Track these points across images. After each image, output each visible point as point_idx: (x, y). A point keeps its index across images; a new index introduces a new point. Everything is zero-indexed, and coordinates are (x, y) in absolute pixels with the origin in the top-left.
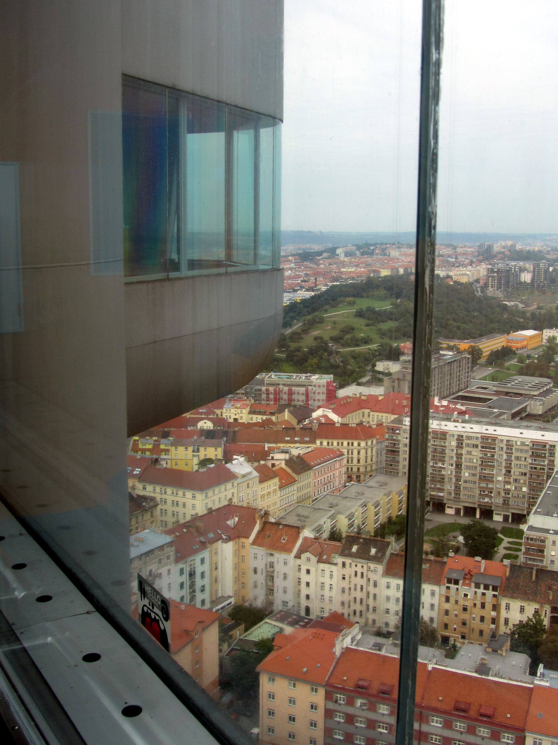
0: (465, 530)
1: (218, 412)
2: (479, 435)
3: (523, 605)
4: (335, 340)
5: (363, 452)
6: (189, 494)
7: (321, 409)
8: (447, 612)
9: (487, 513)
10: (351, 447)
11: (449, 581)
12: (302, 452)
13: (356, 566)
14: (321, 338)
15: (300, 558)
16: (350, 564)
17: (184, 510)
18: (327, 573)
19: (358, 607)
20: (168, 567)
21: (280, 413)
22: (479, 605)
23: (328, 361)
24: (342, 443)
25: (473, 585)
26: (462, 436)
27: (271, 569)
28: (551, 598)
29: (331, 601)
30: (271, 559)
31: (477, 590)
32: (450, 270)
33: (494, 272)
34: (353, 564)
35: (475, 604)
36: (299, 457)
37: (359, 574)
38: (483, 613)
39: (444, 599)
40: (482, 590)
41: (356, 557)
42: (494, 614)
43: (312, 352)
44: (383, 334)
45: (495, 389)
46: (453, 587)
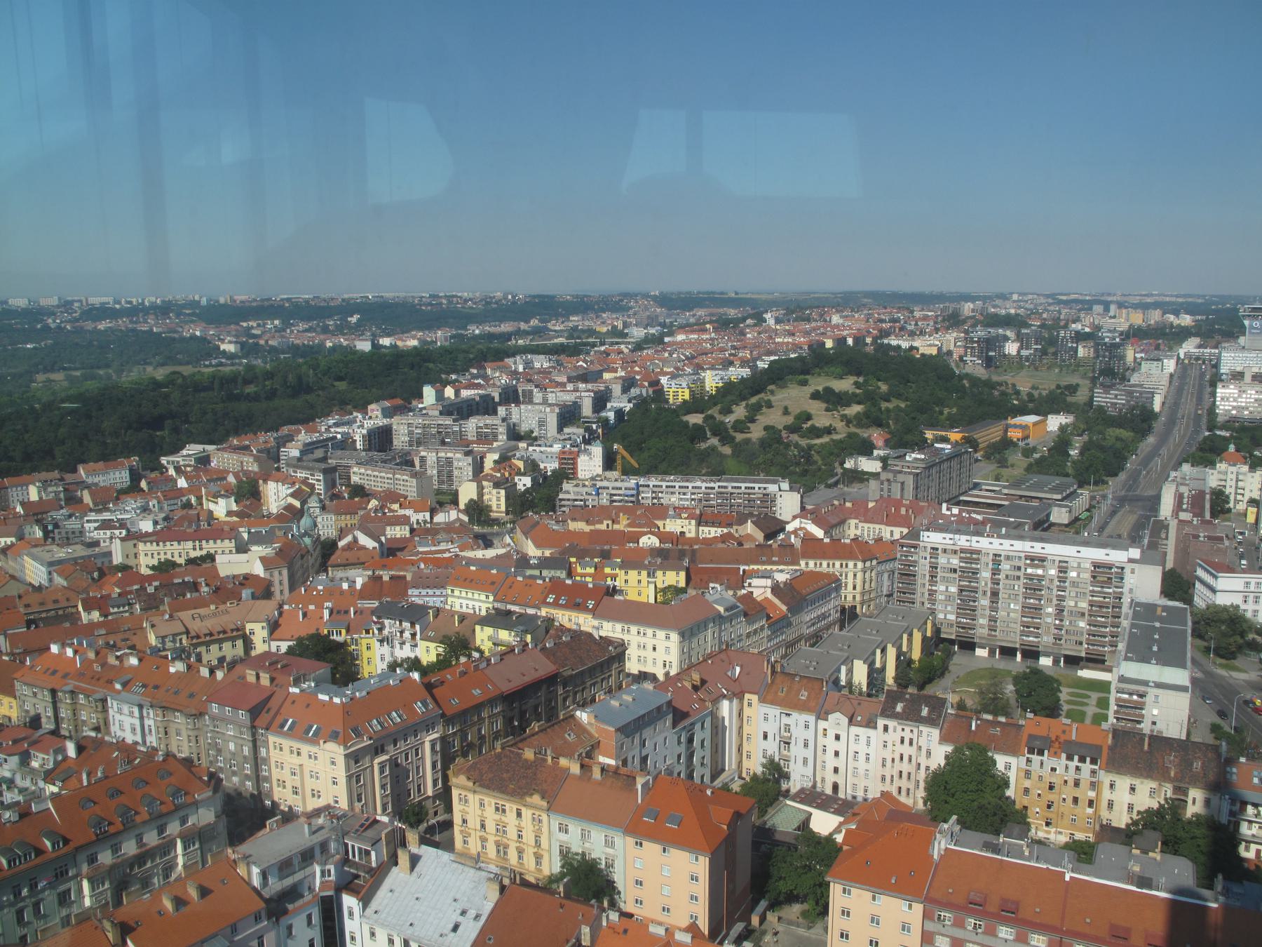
0: (1017, 680)
1: (660, 523)
2: (1022, 555)
3: (1134, 783)
4: (792, 429)
5: (860, 575)
6: (661, 634)
7: (798, 520)
8: (1026, 791)
9: (1032, 654)
11: (1031, 751)
12: (788, 576)
13: (903, 730)
14: (773, 427)
15: (827, 720)
17: (654, 654)
18: (863, 739)
19: (904, 784)
20: (663, 735)
21: (740, 524)
22: (1071, 783)
24: (834, 564)
25: (1064, 756)
26: (1000, 556)
27: (787, 734)
28: (1172, 774)
29: (866, 775)
30: (785, 720)
31: (1069, 763)
32: (913, 340)
36: (785, 583)
37: (907, 741)
39: (1022, 774)
40: (1076, 762)
41: (902, 719)
42: (1092, 794)
43: (764, 444)
44: (848, 420)
45: (1006, 491)
46: (1036, 758)
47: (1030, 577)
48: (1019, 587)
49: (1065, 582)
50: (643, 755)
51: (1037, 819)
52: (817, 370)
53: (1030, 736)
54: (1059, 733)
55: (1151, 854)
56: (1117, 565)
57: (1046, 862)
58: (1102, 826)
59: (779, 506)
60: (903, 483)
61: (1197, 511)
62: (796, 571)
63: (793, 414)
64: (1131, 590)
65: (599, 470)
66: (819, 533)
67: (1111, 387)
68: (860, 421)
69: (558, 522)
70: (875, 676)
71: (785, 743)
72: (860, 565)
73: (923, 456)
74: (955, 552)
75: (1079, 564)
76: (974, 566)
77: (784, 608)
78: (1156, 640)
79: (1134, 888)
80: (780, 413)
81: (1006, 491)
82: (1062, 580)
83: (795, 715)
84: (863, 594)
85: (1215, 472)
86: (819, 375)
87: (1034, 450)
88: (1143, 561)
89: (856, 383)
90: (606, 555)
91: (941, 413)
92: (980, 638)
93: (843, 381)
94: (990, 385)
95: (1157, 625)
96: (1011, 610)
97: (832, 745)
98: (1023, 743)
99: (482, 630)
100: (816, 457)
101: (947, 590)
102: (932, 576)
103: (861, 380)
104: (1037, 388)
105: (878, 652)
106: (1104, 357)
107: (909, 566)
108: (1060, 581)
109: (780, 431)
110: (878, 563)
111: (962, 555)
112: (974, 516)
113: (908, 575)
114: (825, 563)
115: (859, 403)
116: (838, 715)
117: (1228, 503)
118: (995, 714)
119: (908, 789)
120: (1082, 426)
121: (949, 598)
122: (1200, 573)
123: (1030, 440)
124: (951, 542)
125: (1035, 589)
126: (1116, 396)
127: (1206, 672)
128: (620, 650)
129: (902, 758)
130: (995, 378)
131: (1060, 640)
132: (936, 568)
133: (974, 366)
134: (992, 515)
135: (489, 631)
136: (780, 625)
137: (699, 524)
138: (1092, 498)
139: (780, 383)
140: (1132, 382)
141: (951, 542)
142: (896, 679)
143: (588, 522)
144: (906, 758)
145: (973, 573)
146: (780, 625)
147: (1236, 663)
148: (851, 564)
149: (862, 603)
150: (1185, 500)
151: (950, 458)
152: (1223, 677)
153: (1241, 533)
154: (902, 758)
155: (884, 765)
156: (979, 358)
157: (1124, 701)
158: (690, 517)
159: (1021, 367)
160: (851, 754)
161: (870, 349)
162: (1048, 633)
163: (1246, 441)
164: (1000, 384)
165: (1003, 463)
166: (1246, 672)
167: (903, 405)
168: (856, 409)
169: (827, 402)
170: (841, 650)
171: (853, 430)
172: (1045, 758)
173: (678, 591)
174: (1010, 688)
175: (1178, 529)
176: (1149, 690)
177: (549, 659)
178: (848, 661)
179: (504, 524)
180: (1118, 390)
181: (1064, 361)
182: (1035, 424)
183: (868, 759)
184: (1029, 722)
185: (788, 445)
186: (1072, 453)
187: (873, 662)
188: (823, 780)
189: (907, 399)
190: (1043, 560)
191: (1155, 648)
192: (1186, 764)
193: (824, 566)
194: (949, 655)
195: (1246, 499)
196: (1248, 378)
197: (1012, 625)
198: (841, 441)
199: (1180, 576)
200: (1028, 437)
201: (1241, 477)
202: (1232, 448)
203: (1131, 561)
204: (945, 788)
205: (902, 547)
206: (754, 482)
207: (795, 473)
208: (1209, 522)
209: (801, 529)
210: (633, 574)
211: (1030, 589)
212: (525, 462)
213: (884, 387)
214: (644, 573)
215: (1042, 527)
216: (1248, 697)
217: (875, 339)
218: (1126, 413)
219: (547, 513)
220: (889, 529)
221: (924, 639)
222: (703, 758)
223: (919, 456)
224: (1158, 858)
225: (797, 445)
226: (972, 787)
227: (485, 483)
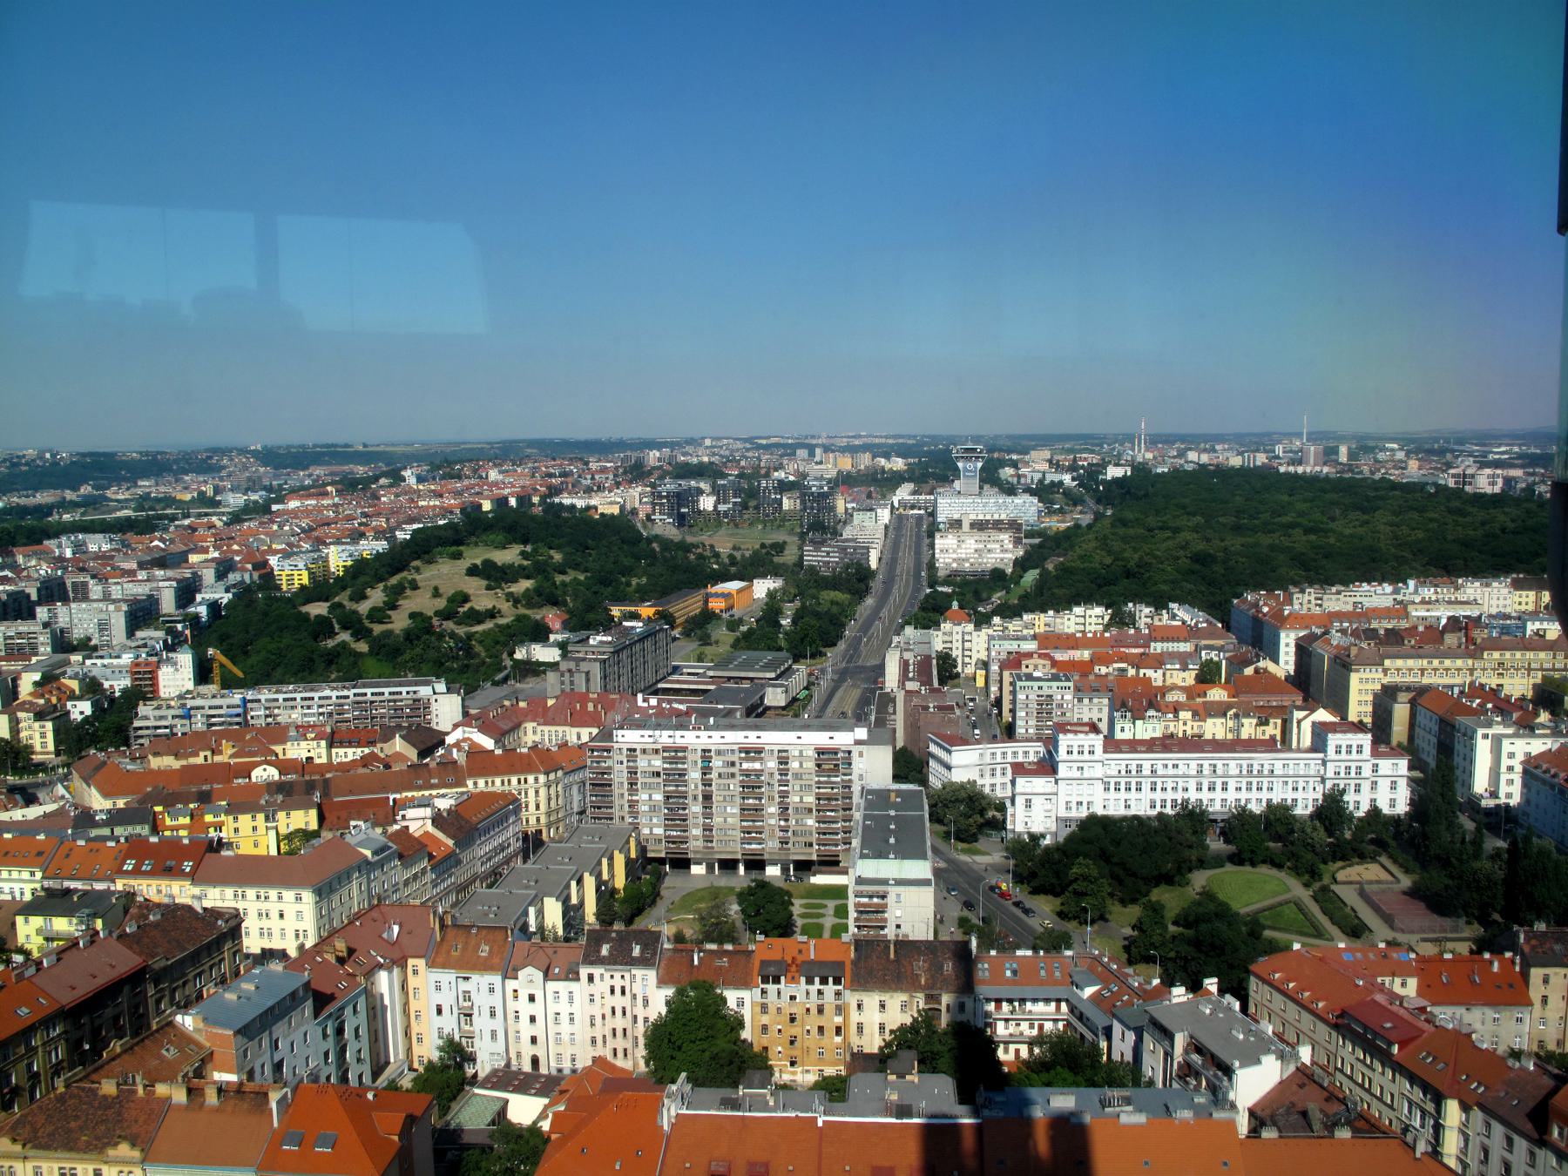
0: (743, 897)
1: (278, 749)
2: (736, 747)
4: (446, 615)
5: (543, 792)
6: (289, 895)
8: (765, 1028)
9: (756, 864)
10: (523, 786)
11: (765, 980)
12: (452, 802)
13: (612, 977)
15: (516, 978)
16: (602, 975)
17: (282, 923)
18: (564, 996)
19: (620, 1043)
20: (303, 1029)
22: (814, 1011)
23: (438, 649)
24: (509, 781)
25: (803, 979)
26: (710, 751)
30: (463, 986)
31: (810, 987)
32: (590, 497)
33: (662, 497)
34: (607, 976)
35: (808, 1010)
36: (449, 811)
37: (618, 991)
38: (822, 1021)
39: (758, 1009)
40: (817, 985)
41: (609, 964)
42: (838, 1020)
43: (410, 636)
44: (515, 600)
45: (711, 673)
46: (771, 988)
47: (747, 773)
48: (735, 786)
49: (786, 775)
50: (277, 1059)
51: (780, 1060)
52: (474, 539)
53: (763, 962)
54: (795, 953)
55: (908, 1077)
56: (843, 748)
57: (795, 1109)
58: (853, 1055)
59: (435, 713)
60: (587, 673)
61: (924, 679)
62: (462, 793)
63: (445, 596)
64: (861, 777)
65: (190, 685)
66: (487, 743)
67: (823, 543)
68: (529, 599)
69: (133, 759)
70: (572, 914)
71: (465, 1015)
72: (542, 778)
73: (610, 639)
74: (656, 751)
75: (801, 752)
76: (680, 766)
77: (450, 842)
78: (891, 831)
79: (894, 1120)
80: (429, 595)
81: (711, 673)
82: (783, 773)
83: (475, 978)
84: (548, 814)
85: (940, 633)
86: (476, 544)
87: (740, 621)
88: (871, 741)
89: (524, 555)
90: (205, 798)
91: (628, 584)
92: (695, 852)
93: (506, 551)
94: (685, 547)
95: (892, 813)
96: (728, 814)
97: (526, 1009)
98: (756, 972)
99: (27, 921)
100: (478, 648)
101: (650, 799)
102: (631, 784)
103: (529, 548)
104: (739, 549)
105: (573, 884)
106: (812, 508)
107: (603, 773)
108: (781, 775)
109: (431, 618)
110: (565, 774)
111: (666, 754)
112: (676, 706)
113: (602, 786)
114: (498, 781)
115: (528, 577)
116: (529, 970)
117: (956, 667)
118: (721, 943)
119: (625, 1050)
120: (793, 591)
121: (653, 809)
122: (933, 749)
123: (735, 610)
124: (651, 740)
125: (753, 787)
126: (828, 553)
127: (947, 861)
128: (233, 923)
129: (614, 1013)
130: (690, 539)
131: (787, 843)
132: (636, 773)
133: (664, 525)
134: (697, 703)
135: (37, 921)
136: (444, 865)
137: (330, 746)
138: (810, 674)
139: (426, 556)
140: (845, 536)
141: (651, 740)
142: (598, 915)
143: (177, 756)
144: (619, 1012)
145: (680, 775)
146: (444, 865)
147: (978, 845)
148: (531, 779)
149: (549, 826)
150: (911, 668)
151: (643, 638)
152: (966, 863)
153: (972, 700)
154: (614, 1013)
155: (592, 1025)
156: (670, 516)
157: (864, 905)
158: (317, 738)
159: (719, 524)
160: (551, 1017)
161: (538, 510)
162: (772, 835)
163: (969, 596)
164: (697, 546)
165: (705, 640)
166: (988, 854)
167: (582, 577)
168: (525, 585)
169: (488, 578)
170: (527, 887)
171: (523, 611)
172: (782, 986)
173: (306, 835)
174: (735, 908)
175: (905, 702)
176: (889, 889)
177: (130, 948)
178: (537, 900)
179: (53, 769)
180: (829, 546)
181: (768, 516)
182: (739, 591)
183: (572, 1020)
184: (761, 946)
185: (441, 636)
186: (783, 622)
187: (568, 898)
188: (519, 1055)
189: (586, 570)
190: (759, 751)
191: (892, 840)
192: (936, 968)
193: (498, 784)
194: (660, 877)
195: (974, 661)
196: (966, 526)
197: (730, 832)
198: (508, 626)
199: (912, 754)
200: (732, 607)
201: (967, 638)
202: (955, 605)
203: (858, 742)
204: (670, 1041)
205: (593, 751)
206: (400, 685)
207: (451, 670)
208: (938, 691)
209: (465, 740)
210: (245, 820)
211: (748, 787)
212: (82, 681)
213: (557, 557)
214: (261, 817)
215: (757, 713)
216: (993, 882)
217: (543, 498)
218: (841, 573)
219: (117, 748)
220: (575, 730)
221: (629, 863)
222: (359, 1051)
223: (605, 639)
224: (916, 1080)
225: (453, 635)
226: (702, 1034)
227: (21, 715)
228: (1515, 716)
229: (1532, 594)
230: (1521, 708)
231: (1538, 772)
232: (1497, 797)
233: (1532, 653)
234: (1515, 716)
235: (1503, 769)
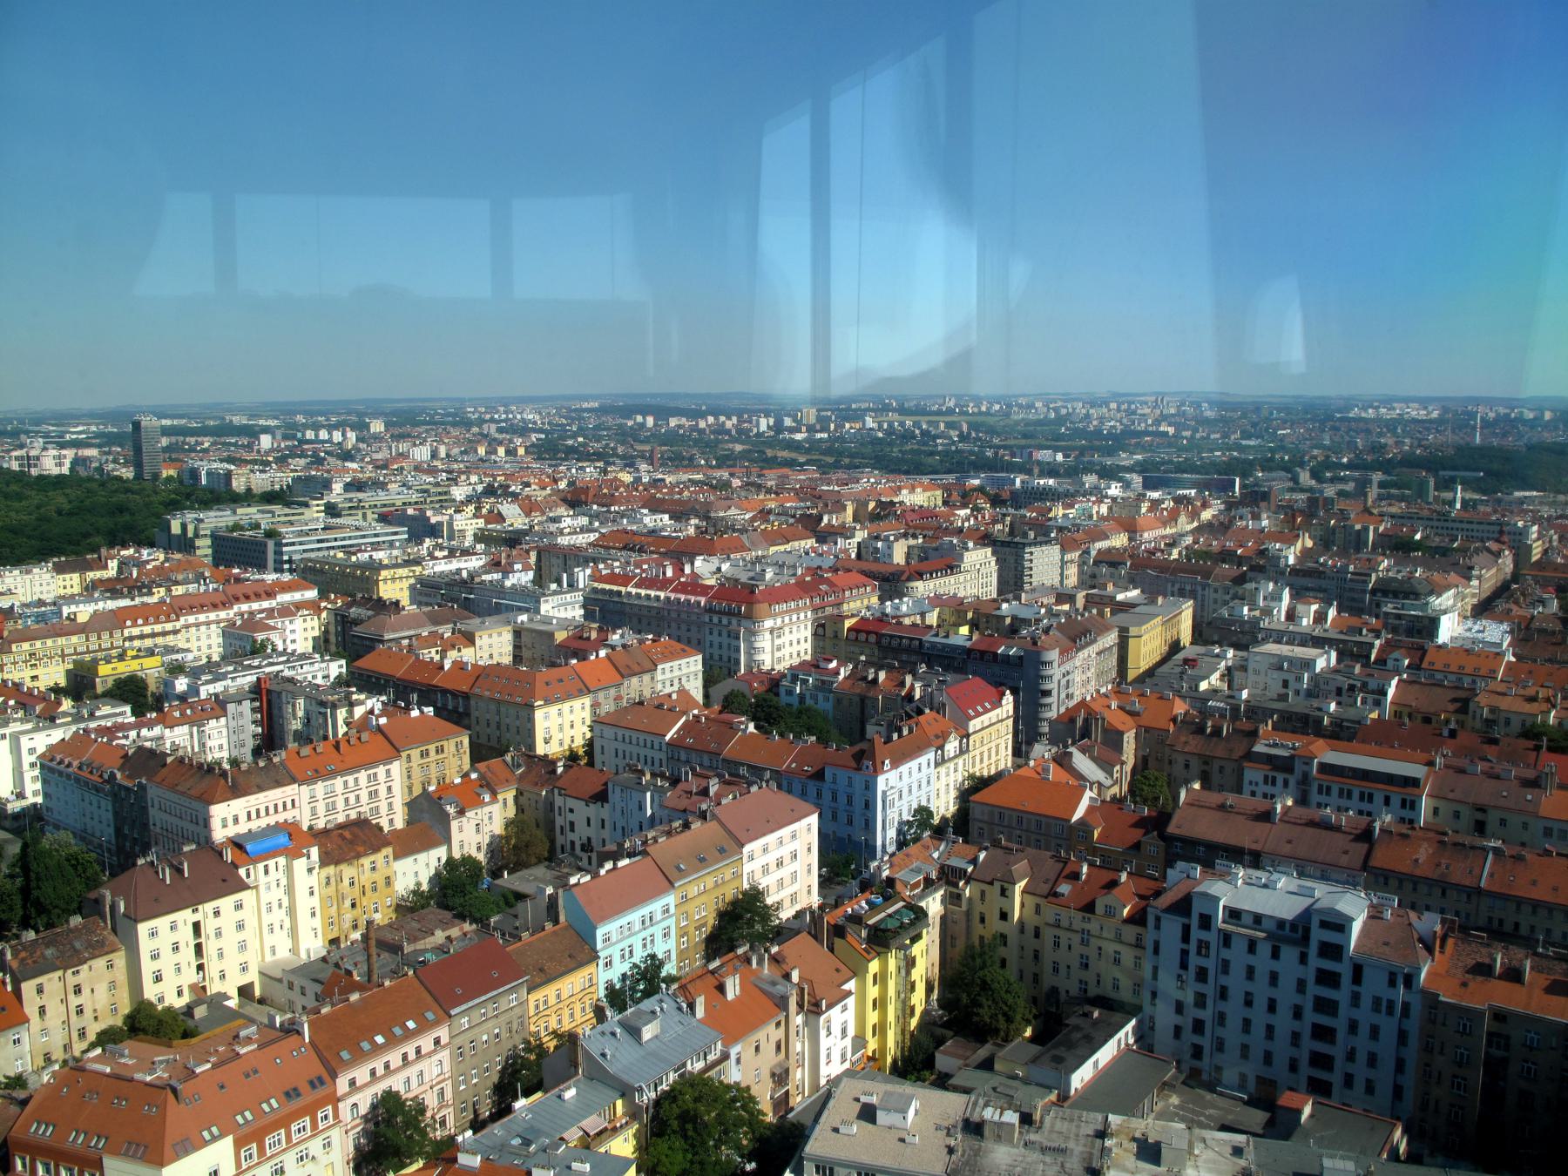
228: (38, 709)
229: (76, 577)
230: (44, 699)
231: (53, 764)
232: (24, 798)
233: (64, 639)
234: (38, 709)
235: (26, 766)
